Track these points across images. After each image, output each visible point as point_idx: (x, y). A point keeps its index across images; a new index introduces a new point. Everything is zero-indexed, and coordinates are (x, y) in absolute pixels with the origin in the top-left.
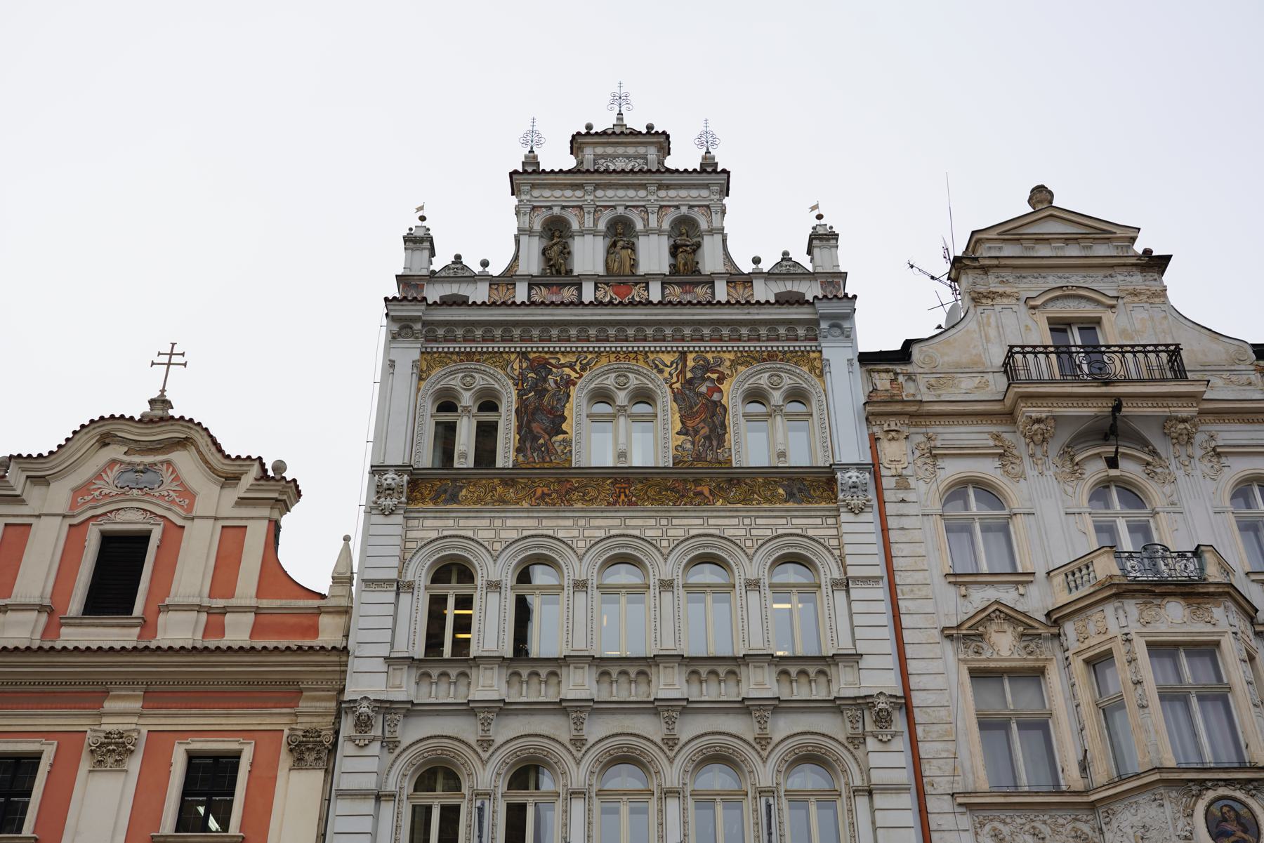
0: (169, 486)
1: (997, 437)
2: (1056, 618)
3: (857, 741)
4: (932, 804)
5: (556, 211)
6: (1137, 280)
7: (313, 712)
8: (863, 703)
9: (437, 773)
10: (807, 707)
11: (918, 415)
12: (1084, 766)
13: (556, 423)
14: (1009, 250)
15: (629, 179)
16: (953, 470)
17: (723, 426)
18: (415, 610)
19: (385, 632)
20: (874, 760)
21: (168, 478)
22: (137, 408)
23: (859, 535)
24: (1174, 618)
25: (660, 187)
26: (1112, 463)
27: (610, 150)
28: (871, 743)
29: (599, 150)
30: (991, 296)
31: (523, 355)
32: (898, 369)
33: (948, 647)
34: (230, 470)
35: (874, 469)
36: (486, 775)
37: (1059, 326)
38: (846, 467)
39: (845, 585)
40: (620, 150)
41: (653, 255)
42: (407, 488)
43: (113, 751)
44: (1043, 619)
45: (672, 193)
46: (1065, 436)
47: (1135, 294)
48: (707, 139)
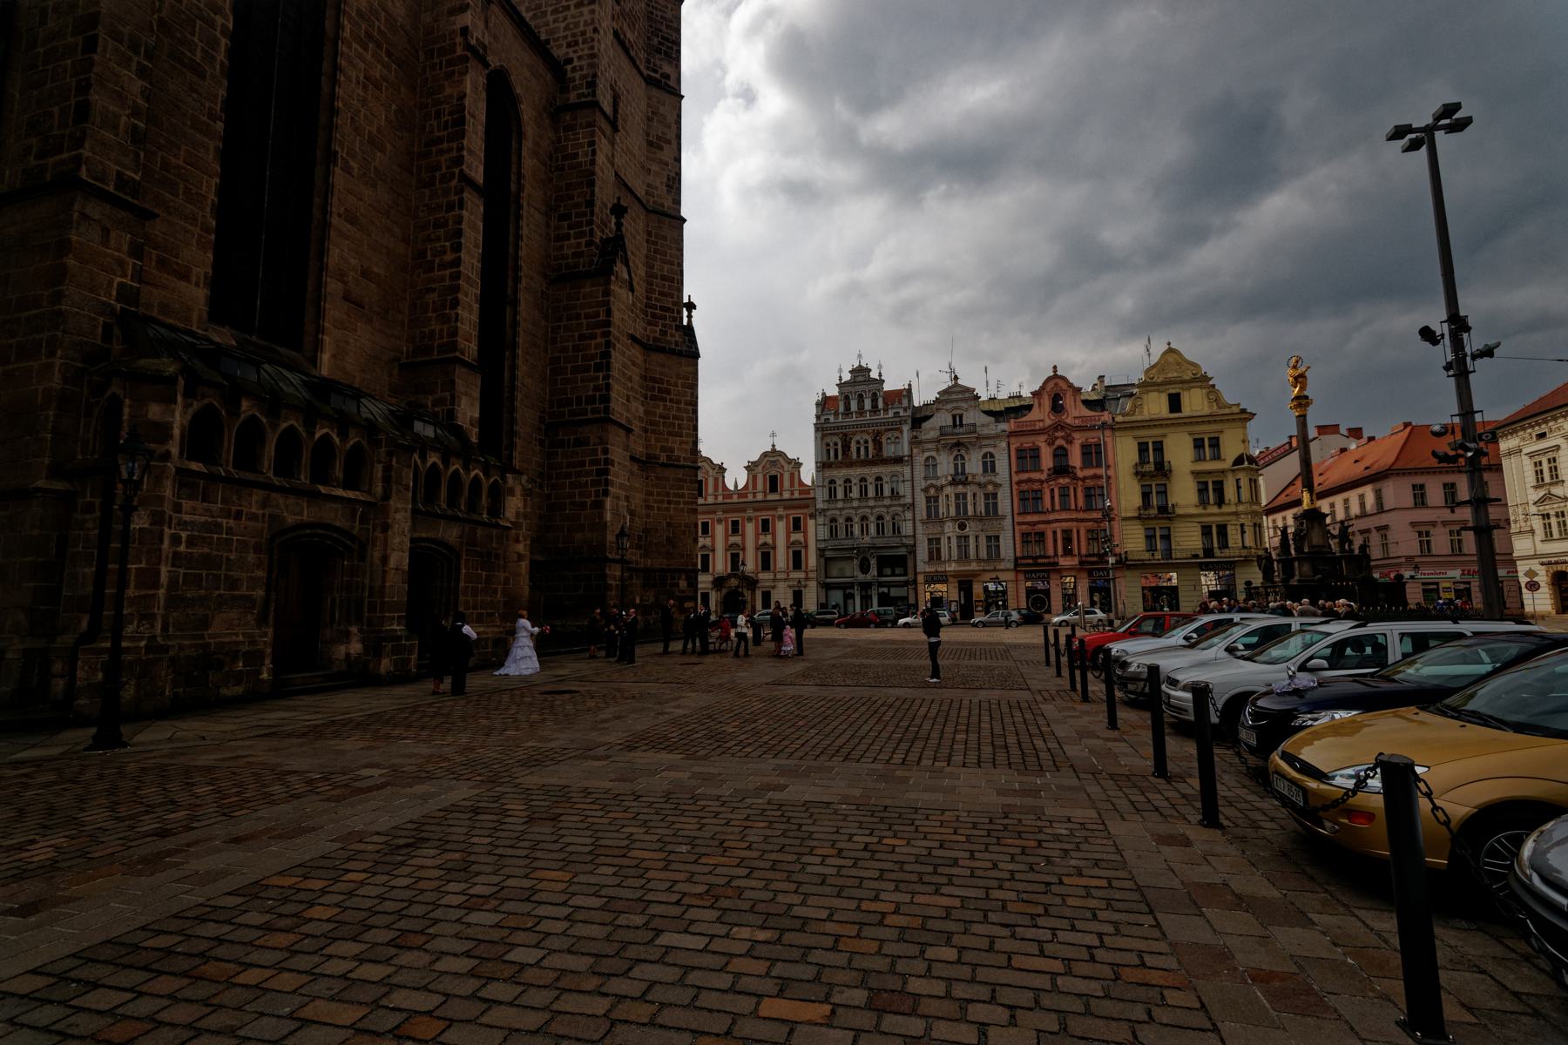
7: (811, 510)
9: (833, 520)
11: (921, 442)
16: (927, 454)
18: (826, 490)
19: (821, 496)
22: (769, 449)
23: (907, 470)
24: (960, 489)
34: (790, 461)
35: (911, 456)
36: (841, 520)
37: (954, 417)
41: (868, 404)
42: (822, 466)
43: (781, 518)
48: (880, 367)
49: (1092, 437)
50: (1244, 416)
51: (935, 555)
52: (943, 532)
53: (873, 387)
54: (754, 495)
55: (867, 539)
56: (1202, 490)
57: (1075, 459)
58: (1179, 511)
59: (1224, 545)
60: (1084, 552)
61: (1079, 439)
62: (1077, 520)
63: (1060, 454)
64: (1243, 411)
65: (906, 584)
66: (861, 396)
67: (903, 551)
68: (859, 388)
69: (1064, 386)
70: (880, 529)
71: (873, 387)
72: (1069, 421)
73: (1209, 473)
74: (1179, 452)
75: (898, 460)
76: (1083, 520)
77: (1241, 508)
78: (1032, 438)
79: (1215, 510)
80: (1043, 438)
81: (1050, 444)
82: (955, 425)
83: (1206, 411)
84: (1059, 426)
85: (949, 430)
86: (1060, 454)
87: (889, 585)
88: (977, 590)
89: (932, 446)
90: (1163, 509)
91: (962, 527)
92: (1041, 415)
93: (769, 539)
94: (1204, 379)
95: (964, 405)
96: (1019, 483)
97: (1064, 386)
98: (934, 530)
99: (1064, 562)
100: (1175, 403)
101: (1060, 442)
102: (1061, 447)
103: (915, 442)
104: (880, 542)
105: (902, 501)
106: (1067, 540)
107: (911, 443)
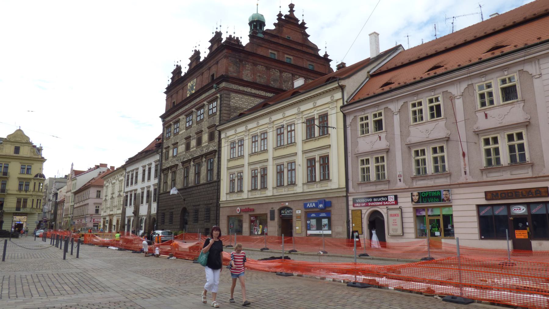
50: (43, 160)
56: (21, 185)
58: (9, 192)
59: (25, 206)
64: (43, 158)
77: (34, 193)
79: (24, 193)
83: (29, 155)
94: (31, 143)
100: (17, 150)
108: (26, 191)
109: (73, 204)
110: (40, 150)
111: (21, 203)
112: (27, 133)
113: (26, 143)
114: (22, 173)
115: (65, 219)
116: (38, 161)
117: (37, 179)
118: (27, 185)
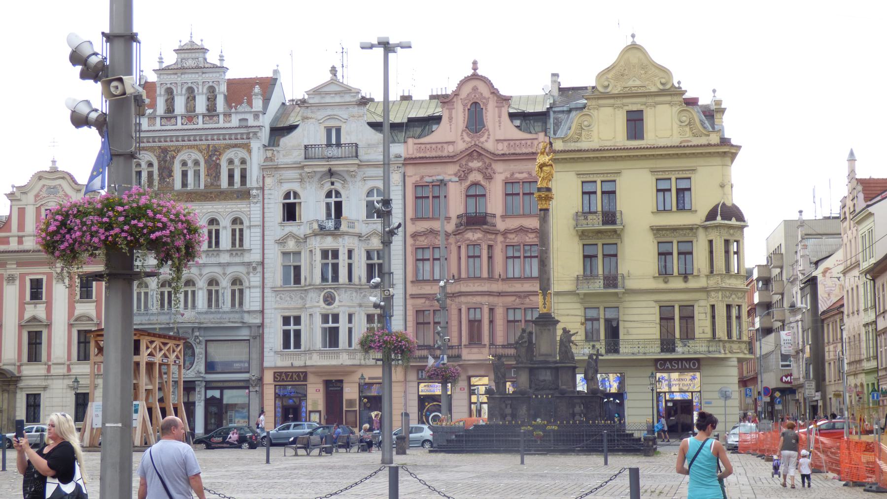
0: (61, 194)
1: (301, 175)
2: (306, 237)
3: (248, 273)
4: (266, 290)
5: (169, 86)
6: (356, 110)
8: (249, 264)
10: (236, 264)
11: (277, 168)
12: (306, 279)
13: (170, 174)
14: (316, 100)
15: (192, 71)
16: (287, 187)
17: (220, 172)
20: (252, 279)
21: (60, 190)
22: (47, 168)
23: (255, 210)
25: (203, 73)
26: (333, 184)
27: (186, 55)
28: (251, 275)
29: (183, 55)
30: (307, 118)
31: (160, 147)
32: (274, 149)
33: (276, 245)
35: (263, 189)
37: (329, 130)
38: (253, 189)
39: (250, 227)
40: (190, 55)
41: (201, 105)
44: (302, 236)
45: (207, 75)
46: (319, 176)
47: (353, 116)
49: (521, 171)
50: (726, 151)
51: (291, 339)
52: (304, 308)
53: (210, 77)
54: (20, 240)
55: (189, 315)
56: (664, 255)
57: (495, 204)
58: (631, 284)
59: (688, 335)
60: (500, 339)
61: (502, 172)
62: (490, 294)
63: (475, 193)
64: (725, 142)
65: (245, 385)
66: (190, 90)
67: (244, 334)
68: (189, 78)
69: (486, 92)
70: (213, 297)
71: (210, 77)
72: (490, 146)
73: (674, 229)
74: (637, 197)
75: (244, 195)
76: (500, 294)
78: (438, 169)
80: (452, 169)
81: (462, 179)
82: (329, 145)
83: (676, 140)
84: (475, 153)
85: (318, 152)
86: (475, 193)
87: (222, 387)
88: (350, 392)
89: (293, 174)
90: (611, 281)
91: (329, 300)
92: (451, 133)
93: (39, 311)
95: (343, 113)
96: (415, 236)
97: (486, 92)
98: (291, 304)
99: (470, 355)
100: (635, 123)
101: (475, 177)
102: (476, 184)
103: (270, 167)
104: (209, 320)
105: (247, 258)
106: (475, 326)
107: (263, 168)
108: (685, 277)
109: (871, 316)
110: (712, 114)
111: (676, 321)
112: (658, 57)
113: (662, 93)
114: (663, 210)
115: (852, 381)
116: (710, 154)
117: (717, 227)
118: (686, 254)
